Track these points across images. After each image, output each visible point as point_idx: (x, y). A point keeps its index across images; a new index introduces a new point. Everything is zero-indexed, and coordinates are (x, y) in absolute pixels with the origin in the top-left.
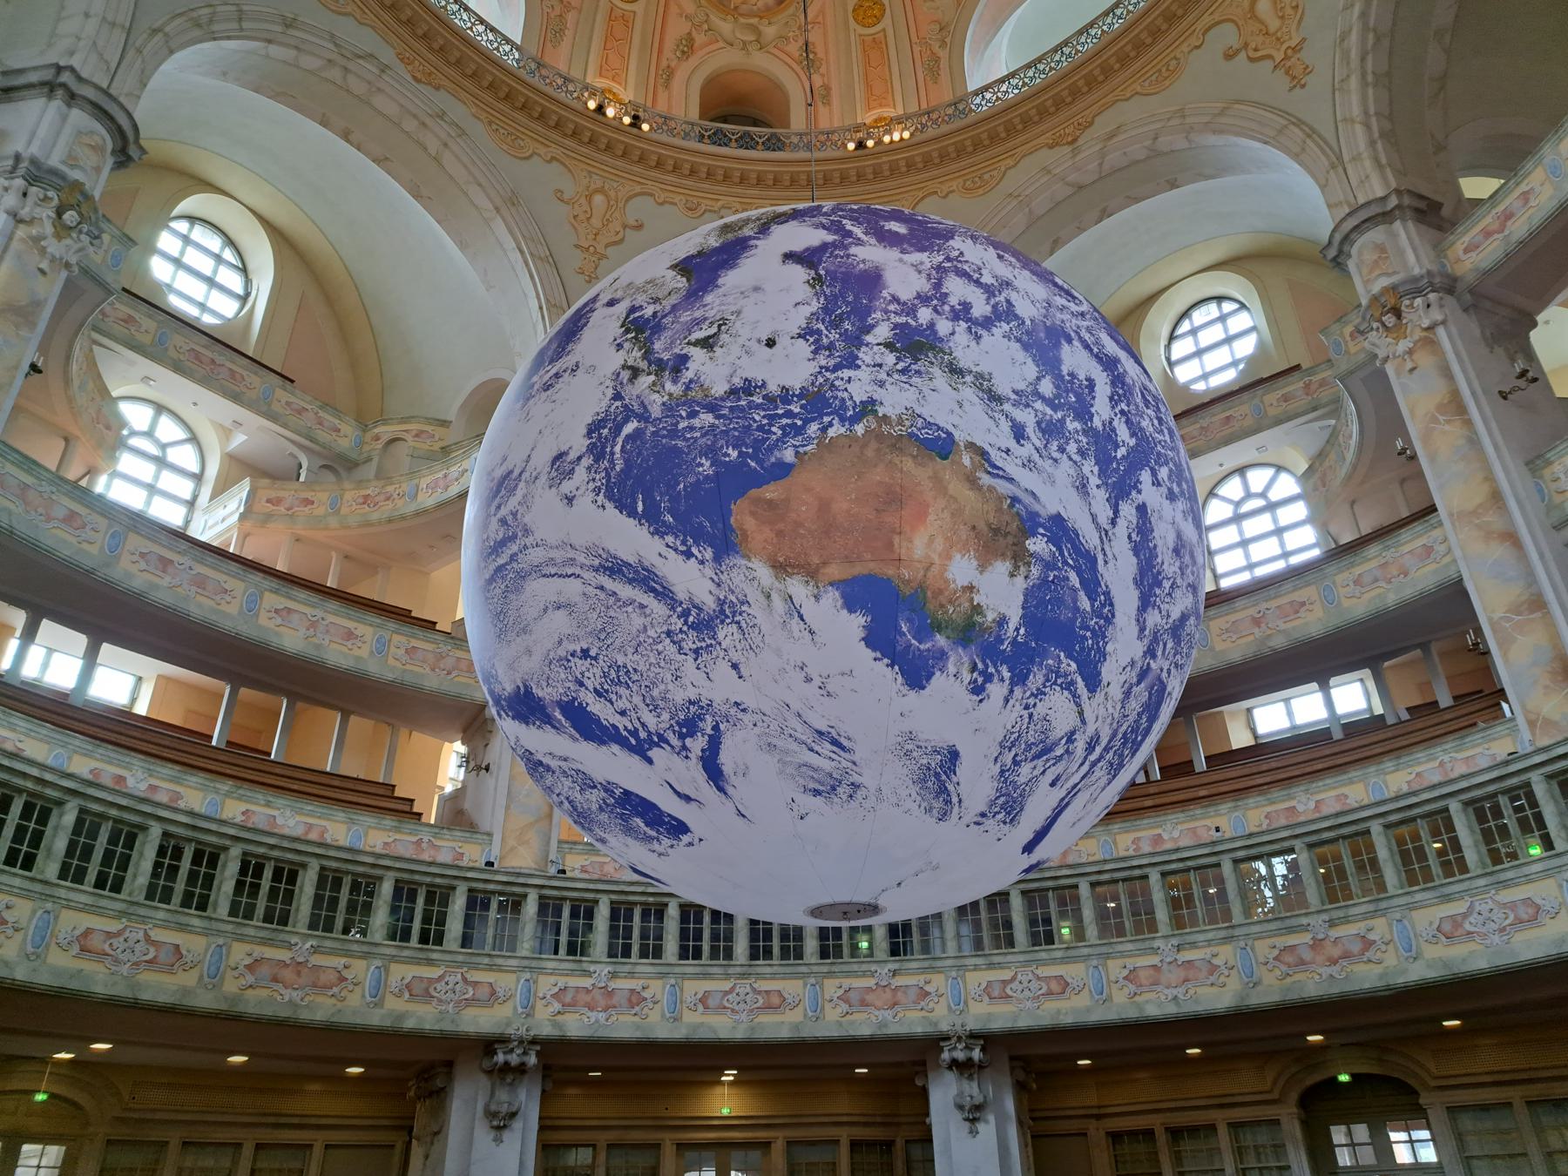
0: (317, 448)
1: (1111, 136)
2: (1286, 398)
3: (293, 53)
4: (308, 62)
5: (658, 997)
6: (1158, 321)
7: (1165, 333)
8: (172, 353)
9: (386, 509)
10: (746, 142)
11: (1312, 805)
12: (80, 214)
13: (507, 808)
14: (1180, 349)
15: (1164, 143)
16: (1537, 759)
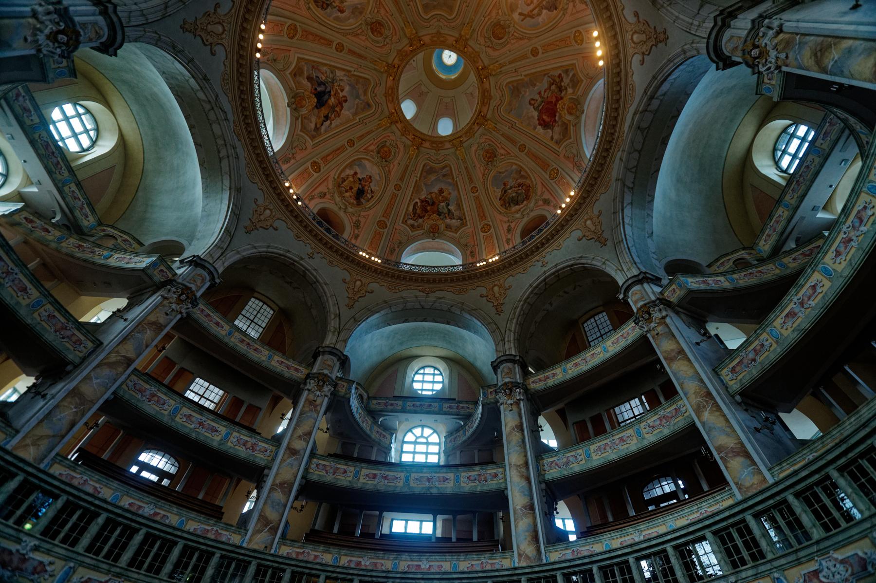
0: (70, 215)
1: (440, 298)
2: (450, 407)
3: (198, 87)
4: (201, 95)
5: (55, 573)
6: (415, 365)
7: (416, 369)
8: (36, 136)
9: (88, 256)
10: (328, 230)
11: (428, 566)
12: (68, 41)
13: (41, 421)
14: (418, 377)
15: (453, 309)
16: (527, 571)
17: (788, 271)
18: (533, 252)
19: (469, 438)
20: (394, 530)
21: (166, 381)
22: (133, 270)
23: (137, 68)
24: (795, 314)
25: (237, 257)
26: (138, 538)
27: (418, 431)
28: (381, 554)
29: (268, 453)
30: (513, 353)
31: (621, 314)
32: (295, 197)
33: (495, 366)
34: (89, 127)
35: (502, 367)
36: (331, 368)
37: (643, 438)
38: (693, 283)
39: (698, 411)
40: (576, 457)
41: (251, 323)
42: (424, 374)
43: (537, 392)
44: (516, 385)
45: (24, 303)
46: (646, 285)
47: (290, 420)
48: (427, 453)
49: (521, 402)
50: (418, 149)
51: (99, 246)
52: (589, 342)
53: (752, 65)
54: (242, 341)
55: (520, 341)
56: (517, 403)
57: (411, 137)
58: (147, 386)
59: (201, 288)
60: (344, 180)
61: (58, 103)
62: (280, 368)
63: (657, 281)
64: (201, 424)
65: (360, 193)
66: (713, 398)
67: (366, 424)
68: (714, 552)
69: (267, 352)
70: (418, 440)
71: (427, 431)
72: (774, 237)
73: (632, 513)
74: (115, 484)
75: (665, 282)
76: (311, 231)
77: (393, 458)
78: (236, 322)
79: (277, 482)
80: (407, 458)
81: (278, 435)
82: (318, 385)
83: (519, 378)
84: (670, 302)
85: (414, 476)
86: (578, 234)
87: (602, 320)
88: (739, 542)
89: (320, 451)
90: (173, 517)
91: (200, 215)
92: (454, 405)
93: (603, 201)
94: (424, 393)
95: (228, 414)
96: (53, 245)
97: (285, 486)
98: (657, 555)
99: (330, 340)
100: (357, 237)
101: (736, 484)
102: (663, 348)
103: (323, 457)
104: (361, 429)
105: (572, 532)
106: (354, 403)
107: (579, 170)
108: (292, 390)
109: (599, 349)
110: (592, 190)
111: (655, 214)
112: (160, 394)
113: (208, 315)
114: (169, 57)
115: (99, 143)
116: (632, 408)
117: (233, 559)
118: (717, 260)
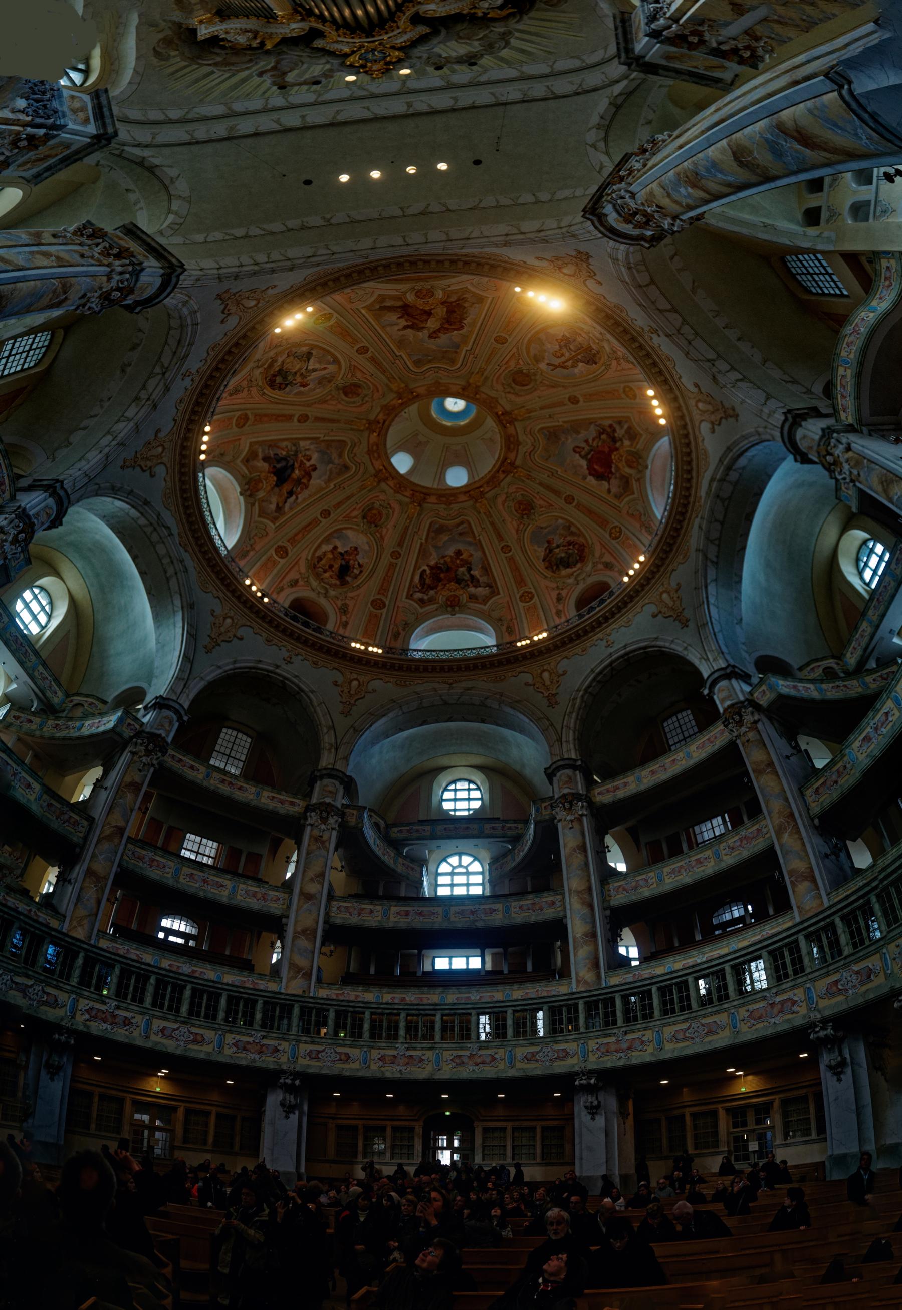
6: (444, 779)
7: (444, 785)
14: (448, 795)
17: (869, 692)
18: (593, 628)
19: (519, 864)
20: (437, 967)
21: (160, 844)
22: (104, 733)
23: (79, 525)
24: (870, 739)
25: (202, 684)
26: (187, 993)
27: (454, 860)
28: (426, 989)
29: (281, 902)
30: (573, 757)
31: (707, 715)
32: (259, 594)
33: (550, 774)
34: (44, 603)
35: (558, 775)
36: (334, 794)
37: (721, 860)
38: (784, 686)
39: (779, 832)
40: (647, 881)
41: (229, 756)
42: (455, 790)
43: (604, 805)
44: (577, 796)
45: (32, 798)
46: (734, 681)
47: (297, 862)
48: (468, 885)
49: (584, 818)
50: (420, 505)
51: (71, 719)
52: (670, 746)
53: (831, 468)
54: (223, 781)
55: (582, 742)
56: (579, 819)
57: (408, 493)
58: (144, 852)
59: (169, 732)
60: (320, 559)
61: (19, 595)
62: (272, 805)
63: (745, 678)
64: (205, 881)
65: (344, 573)
66: (795, 820)
67: (387, 856)
68: (765, 969)
69: (253, 789)
70: (456, 871)
71: (466, 860)
72: (859, 652)
73: (698, 937)
74: (150, 950)
75: (755, 680)
76: (284, 631)
77: (427, 892)
78: (212, 762)
79: (299, 929)
80: (443, 892)
81: (286, 881)
82: (321, 818)
83: (581, 789)
84: (760, 705)
85: (453, 909)
86: (653, 609)
87: (686, 720)
88: (788, 960)
89: (338, 892)
90: (210, 973)
91: (154, 650)
92: (499, 825)
93: (682, 571)
94: (458, 813)
95: (229, 864)
96: (38, 733)
97: (309, 933)
98: (714, 973)
99: (326, 760)
100: (345, 625)
101: (798, 907)
102: (753, 757)
103: (343, 899)
104: (383, 862)
105: (635, 959)
106: (370, 834)
107: (650, 533)
108: (292, 828)
109: (681, 755)
110: (667, 557)
111: (744, 597)
112: (158, 858)
113: (180, 761)
114: (109, 500)
115: (54, 614)
116: (715, 826)
117: (277, 1004)
118: (808, 664)
